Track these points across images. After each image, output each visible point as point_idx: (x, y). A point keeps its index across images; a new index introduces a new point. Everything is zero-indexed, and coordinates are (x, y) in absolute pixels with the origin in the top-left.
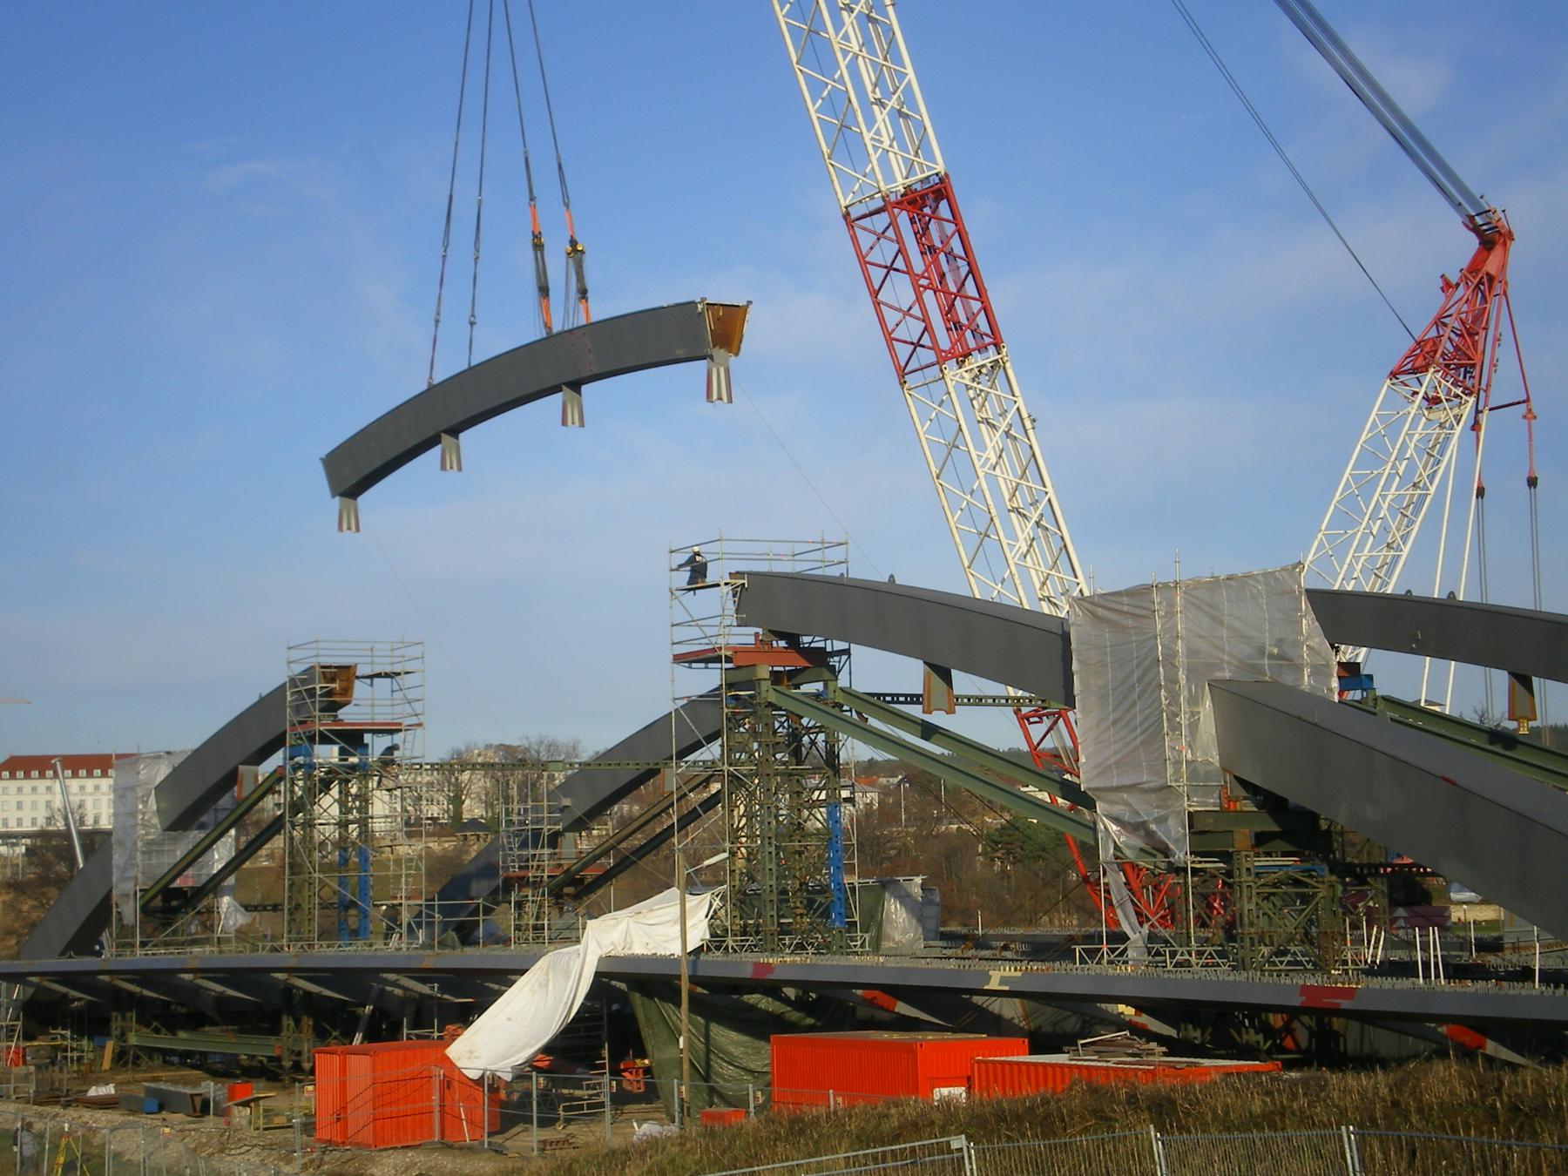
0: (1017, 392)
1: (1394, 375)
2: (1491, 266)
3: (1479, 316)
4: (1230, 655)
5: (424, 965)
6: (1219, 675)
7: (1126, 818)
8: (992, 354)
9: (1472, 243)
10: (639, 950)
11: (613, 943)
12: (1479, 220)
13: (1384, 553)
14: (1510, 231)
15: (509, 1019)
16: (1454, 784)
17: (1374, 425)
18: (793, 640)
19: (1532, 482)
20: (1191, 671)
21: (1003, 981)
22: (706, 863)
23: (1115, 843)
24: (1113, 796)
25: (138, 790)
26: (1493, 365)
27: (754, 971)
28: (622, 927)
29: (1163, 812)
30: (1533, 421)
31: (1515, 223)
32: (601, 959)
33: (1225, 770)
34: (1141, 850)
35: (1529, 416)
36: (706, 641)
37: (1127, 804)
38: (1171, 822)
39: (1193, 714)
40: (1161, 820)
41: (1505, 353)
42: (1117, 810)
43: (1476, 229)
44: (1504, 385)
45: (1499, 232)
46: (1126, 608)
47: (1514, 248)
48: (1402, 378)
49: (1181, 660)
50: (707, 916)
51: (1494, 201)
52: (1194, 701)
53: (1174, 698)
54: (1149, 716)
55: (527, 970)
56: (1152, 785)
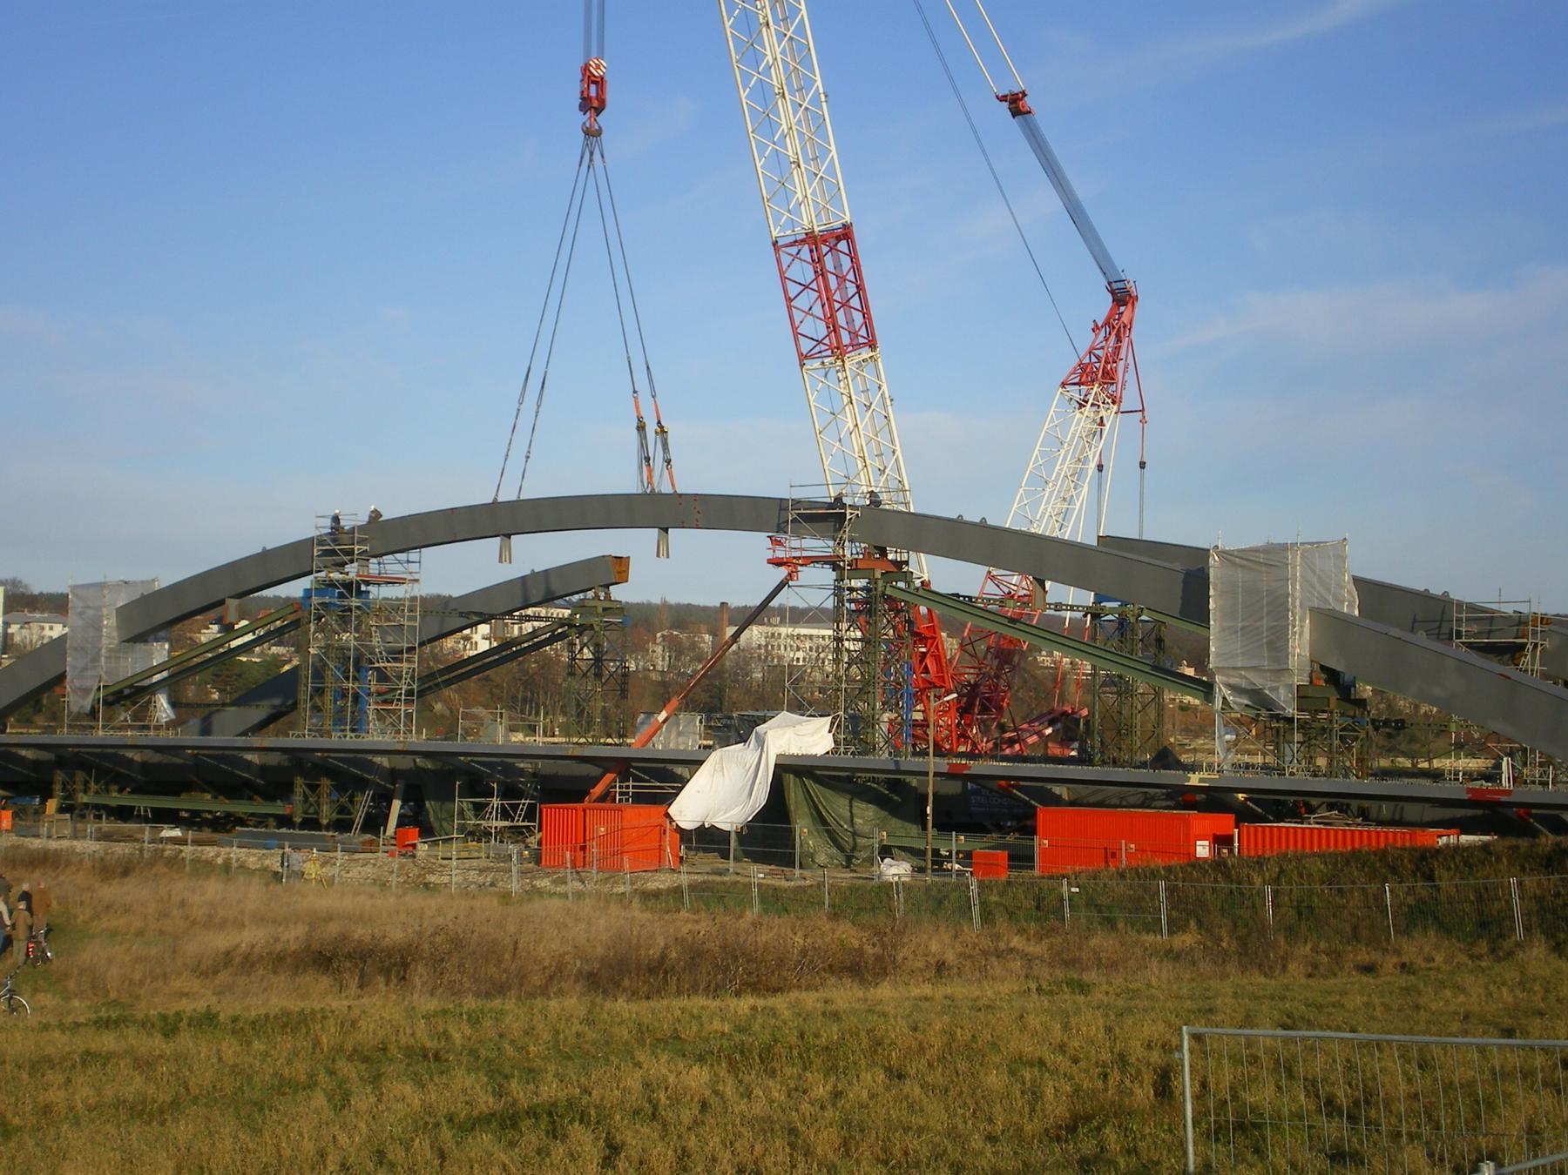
0: (884, 380)
1: (1063, 385)
2: (1125, 319)
3: (1117, 349)
4: (1318, 593)
5: (570, 754)
6: (1311, 604)
7: (1243, 686)
8: (866, 353)
10: (795, 751)
11: (781, 747)
12: (1115, 286)
13: (1058, 506)
16: (1509, 678)
17: (1052, 420)
18: (883, 552)
19: (1142, 465)
21: (1201, 780)
22: (946, 699)
23: (1224, 698)
24: (1231, 672)
26: (1124, 384)
27: (950, 769)
28: (787, 735)
29: (1275, 684)
31: (1141, 290)
32: (779, 756)
33: (1312, 661)
34: (1247, 705)
35: (1143, 421)
36: (830, 550)
37: (1242, 677)
38: (1282, 691)
39: (1302, 627)
40: (1272, 689)
42: (1234, 681)
43: (1112, 292)
44: (1130, 400)
46: (1262, 560)
48: (1068, 388)
49: (1298, 594)
52: (1302, 620)
53: (1293, 616)
55: (701, 763)
56: (1271, 668)
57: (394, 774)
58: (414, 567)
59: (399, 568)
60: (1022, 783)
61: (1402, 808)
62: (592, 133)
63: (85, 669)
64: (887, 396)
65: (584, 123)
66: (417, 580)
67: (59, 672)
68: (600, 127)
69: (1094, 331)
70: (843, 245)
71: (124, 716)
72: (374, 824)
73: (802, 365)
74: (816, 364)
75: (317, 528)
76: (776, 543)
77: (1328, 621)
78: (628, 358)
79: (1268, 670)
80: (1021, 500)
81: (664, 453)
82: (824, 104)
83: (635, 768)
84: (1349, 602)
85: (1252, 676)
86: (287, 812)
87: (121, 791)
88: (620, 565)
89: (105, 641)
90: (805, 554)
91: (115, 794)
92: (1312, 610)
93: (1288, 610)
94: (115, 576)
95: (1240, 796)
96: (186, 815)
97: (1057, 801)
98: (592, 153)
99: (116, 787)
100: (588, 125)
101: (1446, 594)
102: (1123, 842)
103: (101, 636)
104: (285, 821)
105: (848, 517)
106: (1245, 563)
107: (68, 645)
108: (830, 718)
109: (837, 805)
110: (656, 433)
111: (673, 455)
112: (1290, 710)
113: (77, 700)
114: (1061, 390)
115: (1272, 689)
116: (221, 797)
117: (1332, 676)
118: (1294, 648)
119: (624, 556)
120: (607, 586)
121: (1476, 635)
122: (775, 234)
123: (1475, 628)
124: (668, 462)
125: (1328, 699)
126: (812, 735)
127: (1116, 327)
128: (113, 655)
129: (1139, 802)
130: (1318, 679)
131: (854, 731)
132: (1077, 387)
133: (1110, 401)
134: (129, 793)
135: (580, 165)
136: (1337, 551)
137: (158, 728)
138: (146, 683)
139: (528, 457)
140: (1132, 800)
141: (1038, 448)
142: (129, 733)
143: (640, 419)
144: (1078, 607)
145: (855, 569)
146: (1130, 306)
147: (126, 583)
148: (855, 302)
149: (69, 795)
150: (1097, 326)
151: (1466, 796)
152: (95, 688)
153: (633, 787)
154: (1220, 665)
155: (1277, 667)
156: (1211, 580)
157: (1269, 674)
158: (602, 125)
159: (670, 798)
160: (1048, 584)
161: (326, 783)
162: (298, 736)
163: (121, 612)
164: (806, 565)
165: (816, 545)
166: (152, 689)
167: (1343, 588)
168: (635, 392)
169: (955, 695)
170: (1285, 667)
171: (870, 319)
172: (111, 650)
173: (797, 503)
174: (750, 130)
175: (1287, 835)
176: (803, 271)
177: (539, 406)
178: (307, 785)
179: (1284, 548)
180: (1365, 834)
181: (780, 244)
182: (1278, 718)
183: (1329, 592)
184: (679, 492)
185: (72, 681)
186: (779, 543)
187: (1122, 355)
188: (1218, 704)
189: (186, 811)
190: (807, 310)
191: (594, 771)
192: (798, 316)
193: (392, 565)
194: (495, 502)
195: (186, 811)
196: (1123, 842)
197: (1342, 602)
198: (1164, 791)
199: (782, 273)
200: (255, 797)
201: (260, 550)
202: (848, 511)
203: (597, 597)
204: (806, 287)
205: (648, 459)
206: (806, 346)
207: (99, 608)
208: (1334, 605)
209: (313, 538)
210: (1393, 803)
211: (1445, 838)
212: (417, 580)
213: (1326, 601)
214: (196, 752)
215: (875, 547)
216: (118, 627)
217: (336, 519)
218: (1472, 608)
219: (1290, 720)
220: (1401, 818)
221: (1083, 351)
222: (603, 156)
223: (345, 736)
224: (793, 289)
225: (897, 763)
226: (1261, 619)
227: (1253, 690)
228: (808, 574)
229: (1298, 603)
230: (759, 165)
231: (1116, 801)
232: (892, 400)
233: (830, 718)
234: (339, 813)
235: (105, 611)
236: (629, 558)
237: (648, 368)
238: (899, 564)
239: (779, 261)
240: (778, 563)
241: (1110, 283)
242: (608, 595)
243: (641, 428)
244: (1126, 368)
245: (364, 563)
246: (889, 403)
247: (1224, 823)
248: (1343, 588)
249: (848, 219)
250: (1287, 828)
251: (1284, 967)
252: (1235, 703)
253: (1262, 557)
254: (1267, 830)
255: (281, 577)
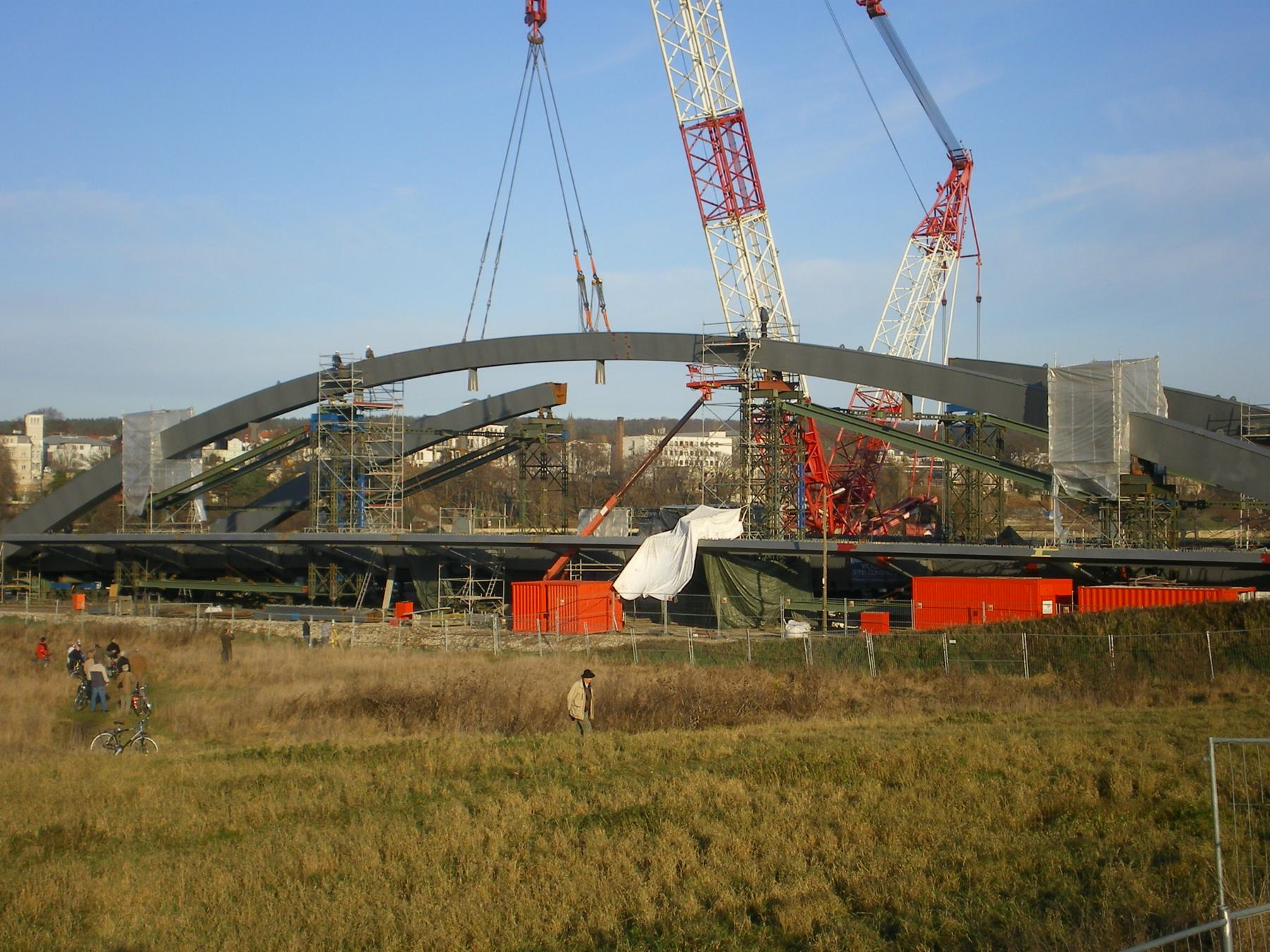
0: (771, 236)
1: (914, 236)
2: (963, 180)
3: (957, 206)
6: (1130, 410)
8: (756, 214)
9: (949, 165)
10: (713, 536)
12: (955, 154)
13: (911, 334)
14: (972, 162)
15: (636, 570)
18: (779, 376)
19: (979, 299)
20: (1123, 408)
21: (1044, 553)
23: (1061, 487)
24: (1066, 466)
25: (151, 433)
26: (963, 233)
29: (1102, 475)
30: (981, 267)
31: (976, 157)
32: (700, 540)
34: (1079, 492)
35: (979, 264)
36: (737, 375)
38: (1108, 480)
40: (1100, 479)
41: (968, 228)
42: (1069, 472)
43: (952, 159)
44: (968, 247)
45: (967, 161)
46: (1090, 375)
47: (975, 172)
48: (918, 238)
50: (740, 520)
51: (965, 145)
52: (1124, 422)
53: (1117, 419)
54: (1100, 429)
55: (639, 546)
57: (387, 560)
58: (397, 395)
59: (386, 396)
60: (896, 558)
61: (1206, 571)
62: (535, 41)
63: (137, 481)
64: (774, 248)
65: (529, 34)
66: (401, 406)
67: (116, 483)
68: (542, 37)
69: (938, 191)
70: (736, 127)
71: (169, 517)
72: (374, 600)
73: (705, 226)
74: (716, 224)
75: (321, 365)
76: (693, 370)
77: (1144, 422)
78: (569, 223)
79: (1097, 464)
80: (881, 330)
81: (600, 299)
82: (720, 12)
83: (582, 552)
84: (1160, 407)
85: (1084, 469)
86: (304, 591)
87: (168, 577)
88: (559, 390)
89: (152, 459)
90: (717, 378)
91: (164, 580)
92: (1132, 414)
93: (1112, 415)
94: (159, 405)
95: (1075, 564)
96: (222, 595)
97: (924, 571)
98: (536, 57)
99: (165, 574)
100: (532, 35)
101: (1233, 398)
102: (984, 603)
103: (149, 455)
104: (300, 599)
105: (751, 348)
106: (1079, 378)
107: (123, 462)
108: (740, 509)
109: (747, 579)
110: (593, 283)
111: (606, 301)
112: (1115, 495)
113: (133, 503)
114: (912, 240)
115: (1100, 479)
116: (250, 581)
117: (1148, 467)
118: (1117, 445)
119: (563, 383)
120: (549, 407)
121: (1258, 431)
122: (681, 119)
123: (1257, 426)
124: (603, 306)
125: (1146, 485)
126: (726, 523)
127: (955, 188)
128: (160, 469)
129: (991, 571)
130: (1137, 469)
131: (757, 518)
132: (925, 237)
133: (952, 248)
134: (175, 578)
135: (527, 68)
136: (1151, 366)
137: (198, 526)
138: (186, 491)
139: (489, 305)
140: (986, 569)
141: (894, 288)
142: (173, 531)
143: (579, 272)
144: (934, 416)
145: (758, 390)
146: (967, 169)
147: (168, 411)
148: (747, 173)
149: (127, 580)
150: (940, 187)
151: (1261, 561)
152: (146, 495)
153: (583, 567)
154: (1057, 461)
155: (1104, 461)
156: (1049, 392)
157: (1097, 467)
158: (543, 34)
159: (615, 575)
160: (914, 398)
161: (334, 568)
162: (311, 531)
163: (168, 436)
164: (714, 388)
165: (727, 371)
166: (191, 496)
167: (1155, 396)
168: (575, 251)
169: (843, 489)
170: (1110, 460)
171: (759, 187)
172: (157, 466)
173: (709, 338)
174: (660, 35)
175: (1117, 595)
176: (704, 149)
177: (497, 265)
178: (319, 570)
179: (1107, 365)
180: (1180, 592)
181: (685, 127)
182: (1104, 501)
183: (1145, 399)
184: (612, 331)
185: (127, 490)
186: (696, 370)
187: (961, 210)
188: (1056, 491)
189: (221, 592)
190: (708, 180)
191: (549, 554)
192: (701, 185)
193: (380, 394)
194: (464, 342)
195: (221, 592)
196: (984, 603)
197: (1154, 407)
198: (1013, 562)
199: (687, 151)
200: (277, 580)
201: (274, 383)
202: (751, 344)
203: (541, 416)
204: (708, 162)
205: (587, 305)
206: (708, 209)
207: (146, 432)
208: (1148, 410)
209: (318, 373)
210: (1198, 568)
211: (1244, 594)
212: (401, 406)
213: (1143, 407)
214: (229, 545)
215: (773, 372)
216: (162, 446)
217: (337, 359)
218: (1256, 409)
219: (1115, 503)
220: (1206, 578)
221: (929, 207)
222: (544, 60)
223: (348, 530)
224: (697, 164)
225: (796, 544)
226: (1090, 422)
227: (1084, 480)
228: (719, 395)
229: (1120, 409)
230: (668, 63)
231: (973, 571)
232: (777, 252)
233: (740, 509)
234: (343, 592)
235: (152, 434)
236: (566, 384)
237: (585, 231)
238: (791, 385)
239: (685, 141)
240: (695, 386)
241: (950, 152)
242: (550, 414)
243: (581, 280)
244: (964, 220)
245: (360, 392)
246: (775, 254)
247: (1065, 587)
248: (1155, 396)
249: (740, 105)
250: (1117, 589)
251: (1131, 698)
252: (1069, 490)
253: (1090, 373)
254: (1101, 591)
255: (295, 405)
